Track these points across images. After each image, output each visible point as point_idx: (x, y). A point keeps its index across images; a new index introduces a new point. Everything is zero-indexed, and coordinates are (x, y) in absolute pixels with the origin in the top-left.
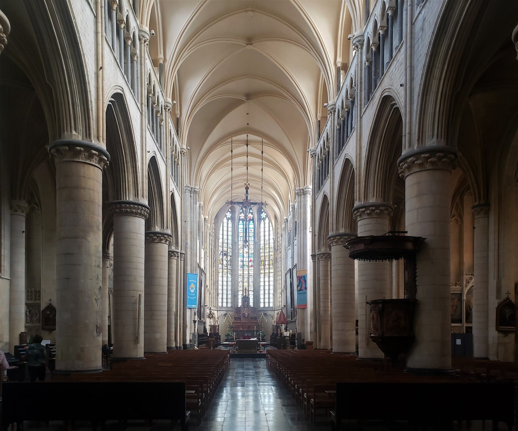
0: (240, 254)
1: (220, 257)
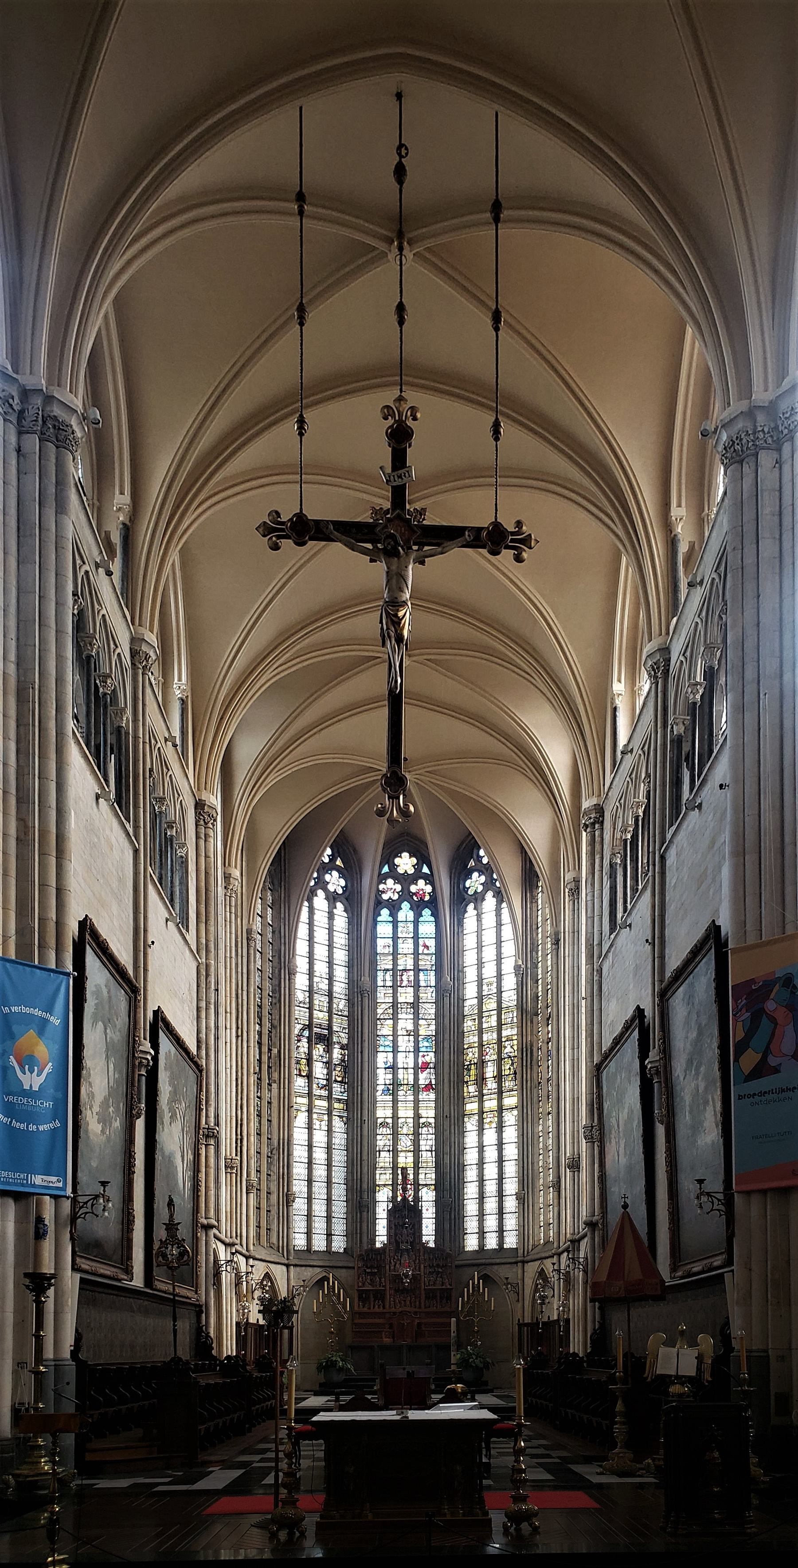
0: (382, 1041)
1: (302, 1050)
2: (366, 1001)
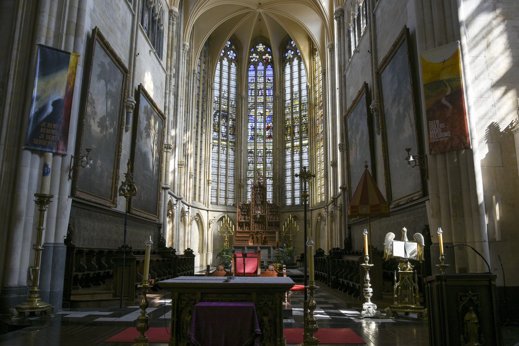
2: (243, 101)
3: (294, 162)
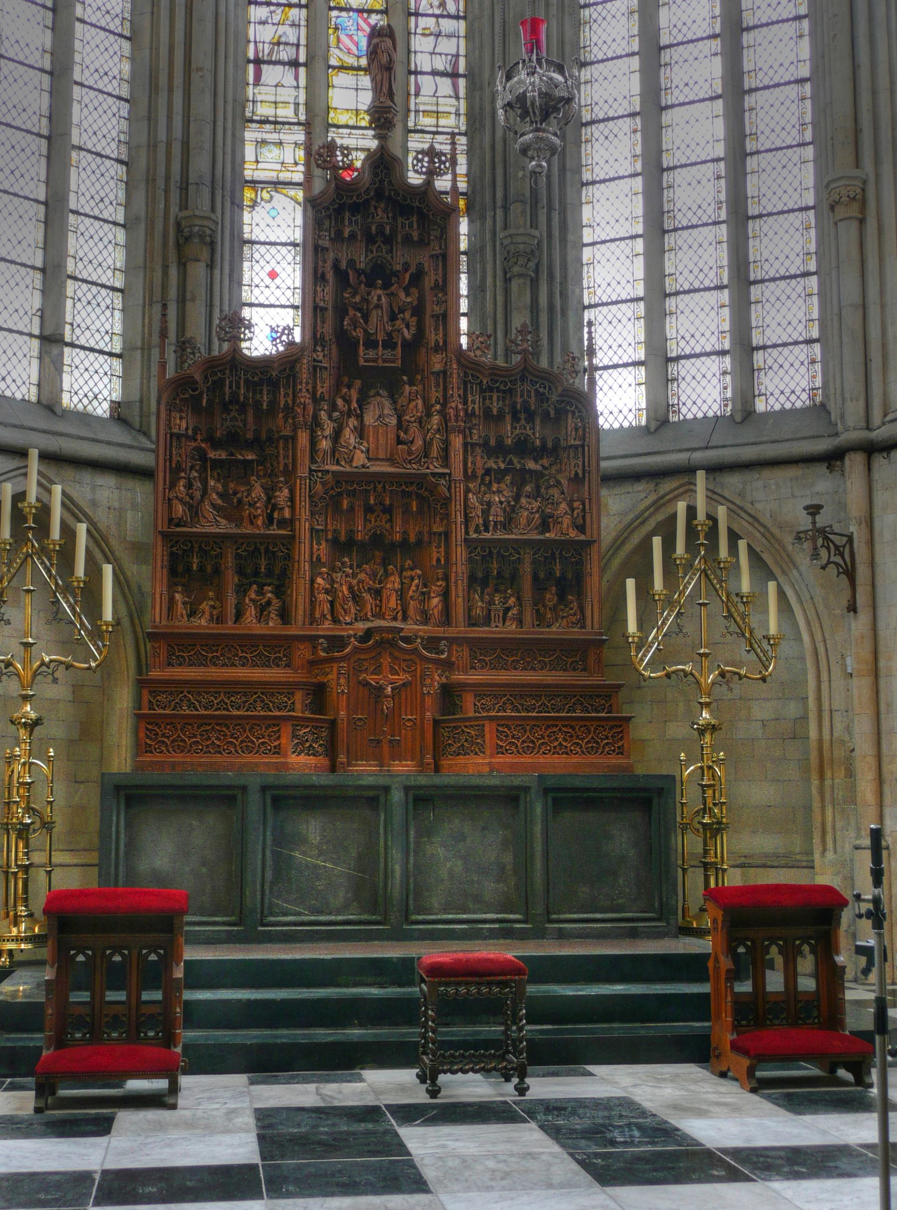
3: (665, 56)
